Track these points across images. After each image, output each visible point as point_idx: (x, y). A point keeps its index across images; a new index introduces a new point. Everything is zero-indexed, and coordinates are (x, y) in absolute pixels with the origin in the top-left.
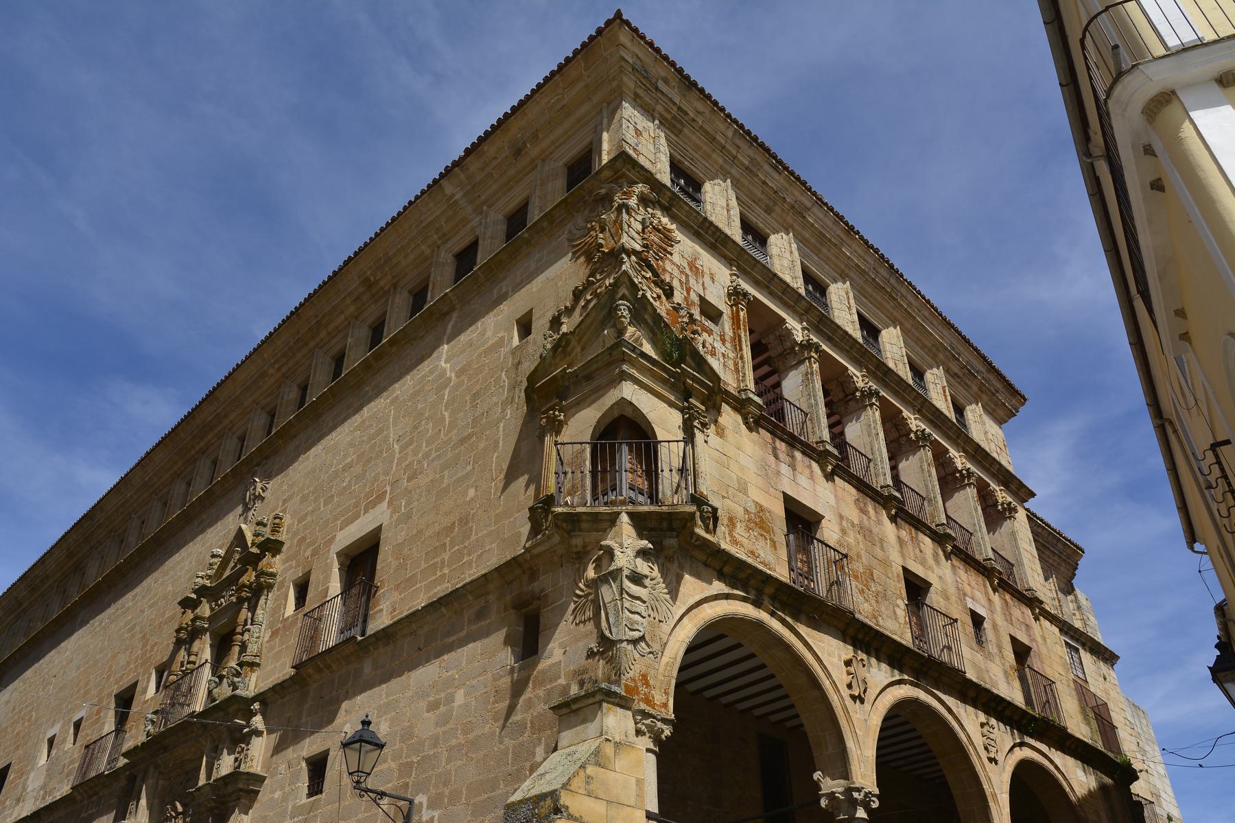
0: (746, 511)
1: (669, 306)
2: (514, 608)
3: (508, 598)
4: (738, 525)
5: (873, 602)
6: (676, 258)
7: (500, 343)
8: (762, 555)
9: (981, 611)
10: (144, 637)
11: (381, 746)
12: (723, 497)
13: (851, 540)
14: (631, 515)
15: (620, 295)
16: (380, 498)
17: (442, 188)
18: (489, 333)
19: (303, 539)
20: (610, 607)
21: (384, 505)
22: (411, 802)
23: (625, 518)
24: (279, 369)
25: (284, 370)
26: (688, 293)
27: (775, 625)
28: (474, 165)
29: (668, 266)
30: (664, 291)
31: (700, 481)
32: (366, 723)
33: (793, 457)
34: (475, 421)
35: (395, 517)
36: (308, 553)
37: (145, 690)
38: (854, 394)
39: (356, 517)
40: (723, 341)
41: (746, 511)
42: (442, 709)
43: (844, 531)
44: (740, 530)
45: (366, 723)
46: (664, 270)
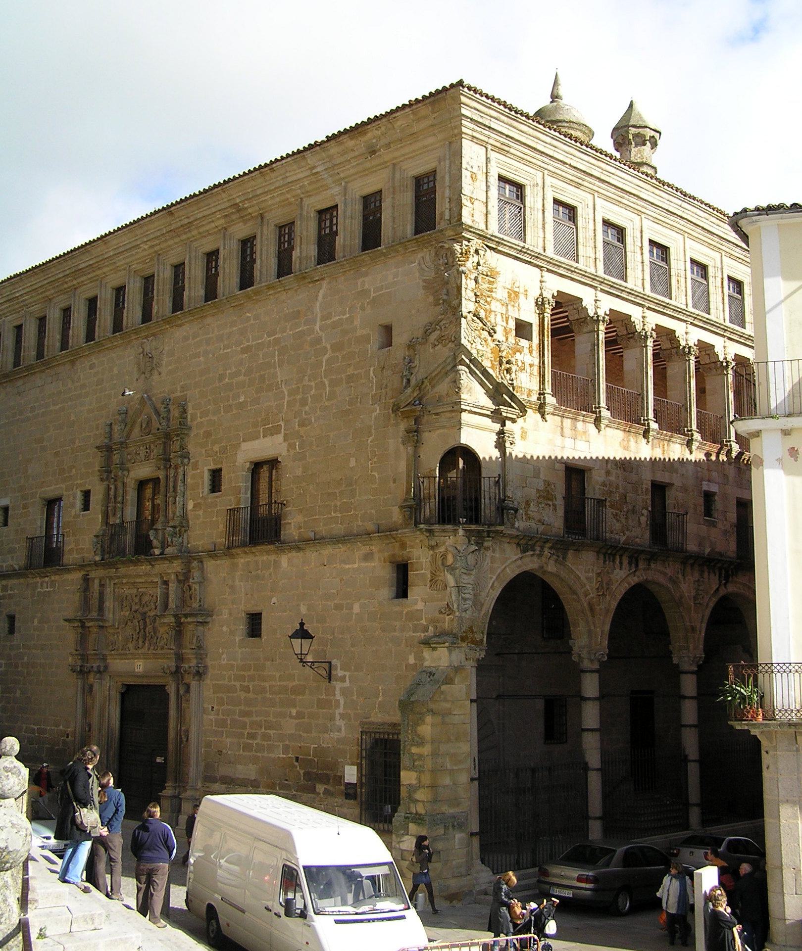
0: (538, 490)
1: (492, 345)
3: (386, 554)
5: (623, 521)
6: (501, 293)
7: (366, 339)
9: (714, 488)
10: (57, 454)
11: (312, 638)
13: (612, 478)
16: (275, 430)
17: (304, 158)
18: (357, 322)
19: (208, 434)
21: (280, 438)
22: (330, 663)
23: (461, 532)
24: (152, 247)
25: (156, 249)
27: (551, 567)
28: (334, 149)
29: (495, 306)
30: (489, 333)
32: (302, 624)
33: (574, 428)
35: (292, 452)
36: (216, 448)
37: (73, 505)
38: (633, 333)
39: (257, 438)
40: (531, 352)
41: (538, 490)
42: (345, 611)
44: (533, 507)
45: (302, 624)
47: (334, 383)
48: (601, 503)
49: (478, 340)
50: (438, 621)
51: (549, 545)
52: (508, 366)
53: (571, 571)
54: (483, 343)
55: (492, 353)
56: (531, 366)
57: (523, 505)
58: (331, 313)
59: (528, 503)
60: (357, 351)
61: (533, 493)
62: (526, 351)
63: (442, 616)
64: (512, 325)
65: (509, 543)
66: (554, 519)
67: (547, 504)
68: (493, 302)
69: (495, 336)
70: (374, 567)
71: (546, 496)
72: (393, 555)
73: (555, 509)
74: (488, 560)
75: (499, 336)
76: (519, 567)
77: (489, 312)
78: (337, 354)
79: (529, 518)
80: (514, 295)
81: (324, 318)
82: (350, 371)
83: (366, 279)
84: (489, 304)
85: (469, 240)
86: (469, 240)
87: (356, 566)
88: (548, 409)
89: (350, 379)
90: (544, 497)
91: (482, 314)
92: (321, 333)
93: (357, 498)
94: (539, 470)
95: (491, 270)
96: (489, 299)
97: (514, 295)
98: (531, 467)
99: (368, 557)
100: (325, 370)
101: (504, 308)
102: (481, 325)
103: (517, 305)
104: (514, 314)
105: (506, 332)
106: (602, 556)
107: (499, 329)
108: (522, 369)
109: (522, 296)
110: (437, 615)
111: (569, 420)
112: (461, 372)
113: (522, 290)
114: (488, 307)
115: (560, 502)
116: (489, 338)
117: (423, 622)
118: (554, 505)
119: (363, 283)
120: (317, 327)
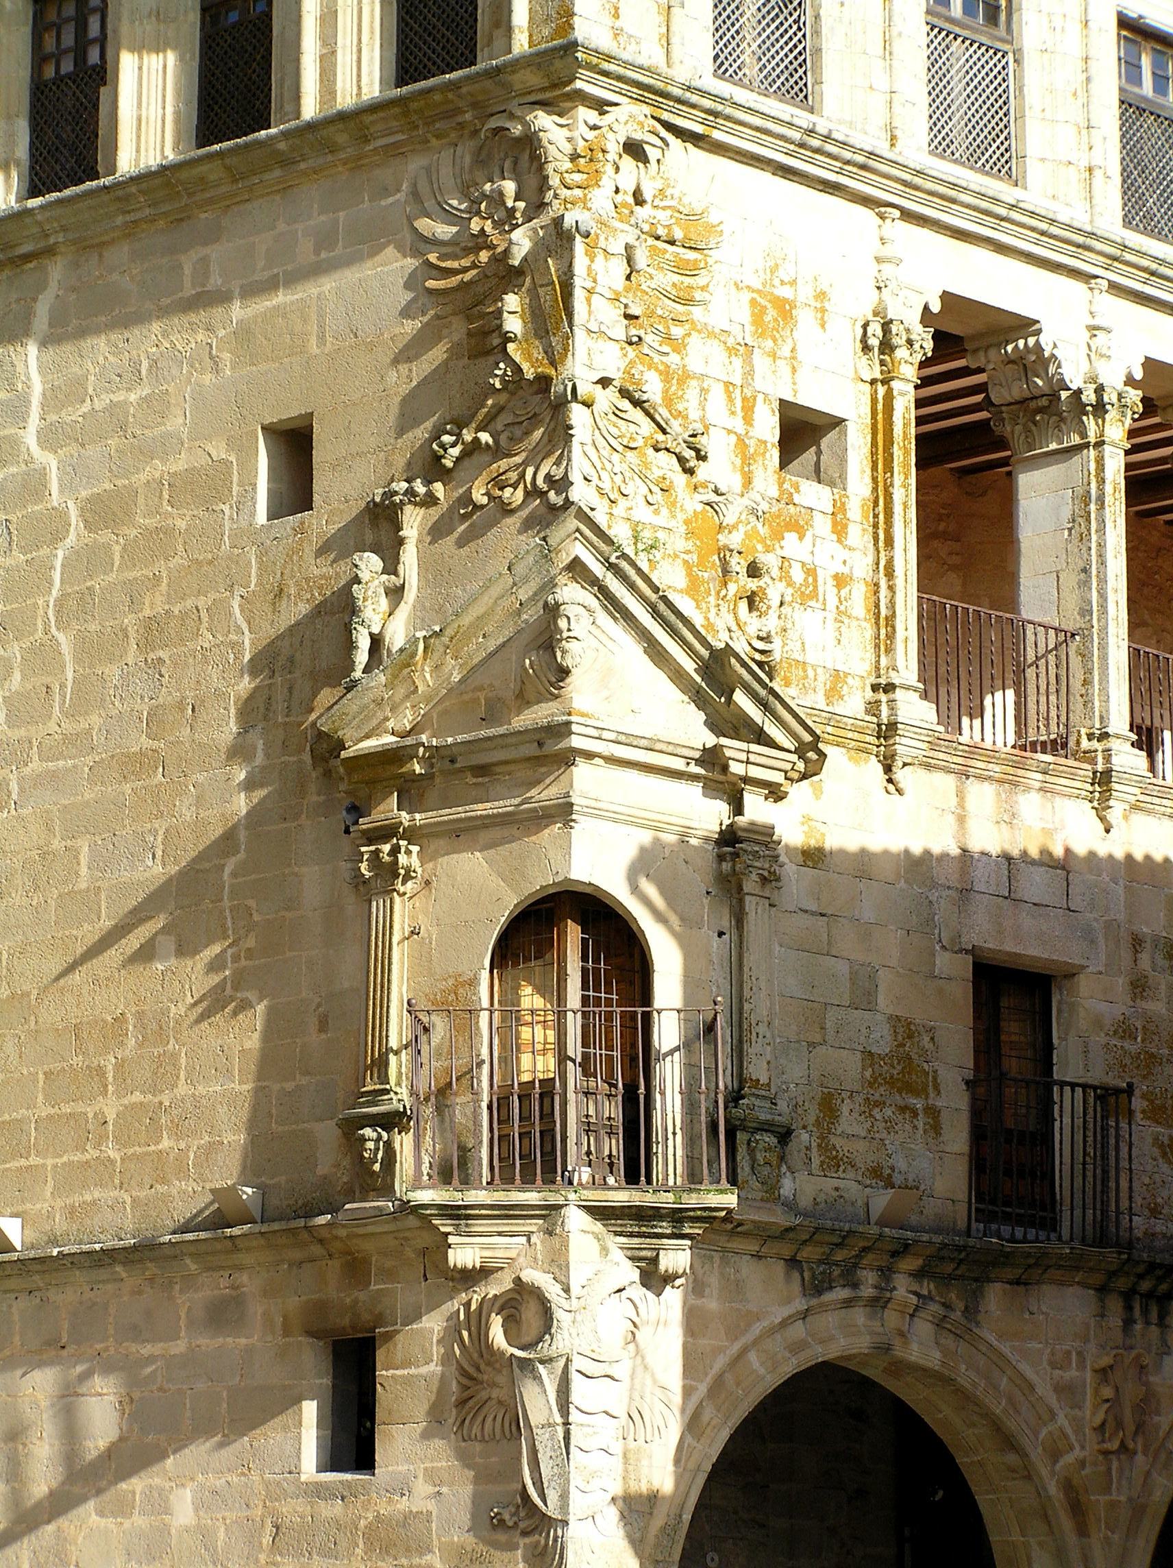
1: (692, 504)
2: (309, 1333)
3: (293, 1303)
4: (845, 1110)
6: (725, 308)
8: (901, 1164)
12: (812, 1045)
15: (564, 559)
20: (542, 1437)
26: (748, 419)
27: (922, 1347)
30: (681, 460)
31: (751, 1051)
34: (155, 721)
40: (840, 529)
43: (1139, 987)
44: (849, 1121)
46: (685, 377)
47: (87, 650)
48: (1109, 1100)
49: (637, 488)
51: (910, 1263)
52: (753, 584)
53: (1000, 1362)
54: (658, 497)
55: (690, 534)
56: (841, 581)
57: (813, 1114)
58: (81, 382)
59: (829, 1107)
60: (181, 524)
61: (850, 1068)
62: (822, 525)
64: (768, 427)
65: (758, 1256)
66: (936, 1167)
67: (903, 1109)
68: (695, 341)
69: (703, 471)
70: (249, 1351)
71: (899, 1076)
72: (320, 1308)
73: (936, 1128)
75: (719, 468)
76: (796, 1347)
77: (676, 378)
78: (105, 536)
79: (834, 1162)
80: (774, 313)
81: (52, 400)
82: (154, 604)
83: (214, 252)
84: (679, 346)
85: (601, 106)
86: (601, 106)
87: (179, 1347)
88: (905, 747)
89: (152, 632)
90: (891, 1082)
91: (653, 389)
92: (50, 461)
93: (182, 1089)
94: (872, 977)
95: (692, 218)
96: (677, 331)
97: (774, 313)
98: (842, 968)
99: (223, 1314)
100: (64, 597)
101: (738, 362)
102: (647, 427)
103: (785, 351)
104: (775, 383)
105: (746, 457)
106: (1115, 1305)
107: (718, 445)
108: (808, 595)
109: (805, 318)
111: (988, 789)
112: (570, 610)
113: (804, 293)
114: (674, 359)
115: (954, 1101)
116: (680, 479)
118: (933, 1112)
119: (203, 268)
120: (30, 438)
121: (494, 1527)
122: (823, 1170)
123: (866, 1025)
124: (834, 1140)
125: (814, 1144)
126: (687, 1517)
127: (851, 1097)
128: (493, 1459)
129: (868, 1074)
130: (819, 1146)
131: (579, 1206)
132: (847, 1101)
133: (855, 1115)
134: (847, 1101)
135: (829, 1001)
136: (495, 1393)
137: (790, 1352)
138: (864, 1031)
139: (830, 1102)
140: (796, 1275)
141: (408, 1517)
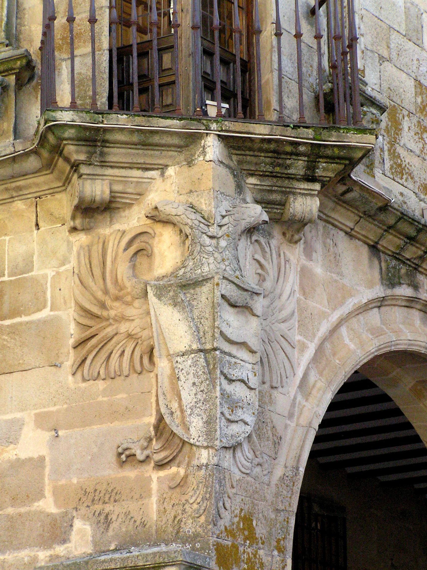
4: (406, 124)
12: (382, 59)
14: (230, 142)
23: (212, 148)
50: (113, 495)
63: (131, 473)
65: (350, 235)
74: (292, 281)
110: (110, 471)
117: (48, 505)
121: (122, 464)
122: (392, 174)
123: (416, 57)
124: (400, 150)
125: (386, 148)
126: (302, 470)
127: (408, 116)
128: (119, 396)
129: (419, 100)
130: (389, 150)
131: (219, 136)
132: (406, 118)
133: (413, 133)
134: (406, 118)
135: (392, 25)
136: (124, 327)
137: (372, 334)
138: (415, 62)
139: (395, 116)
140: (376, 262)
141: (18, 464)
